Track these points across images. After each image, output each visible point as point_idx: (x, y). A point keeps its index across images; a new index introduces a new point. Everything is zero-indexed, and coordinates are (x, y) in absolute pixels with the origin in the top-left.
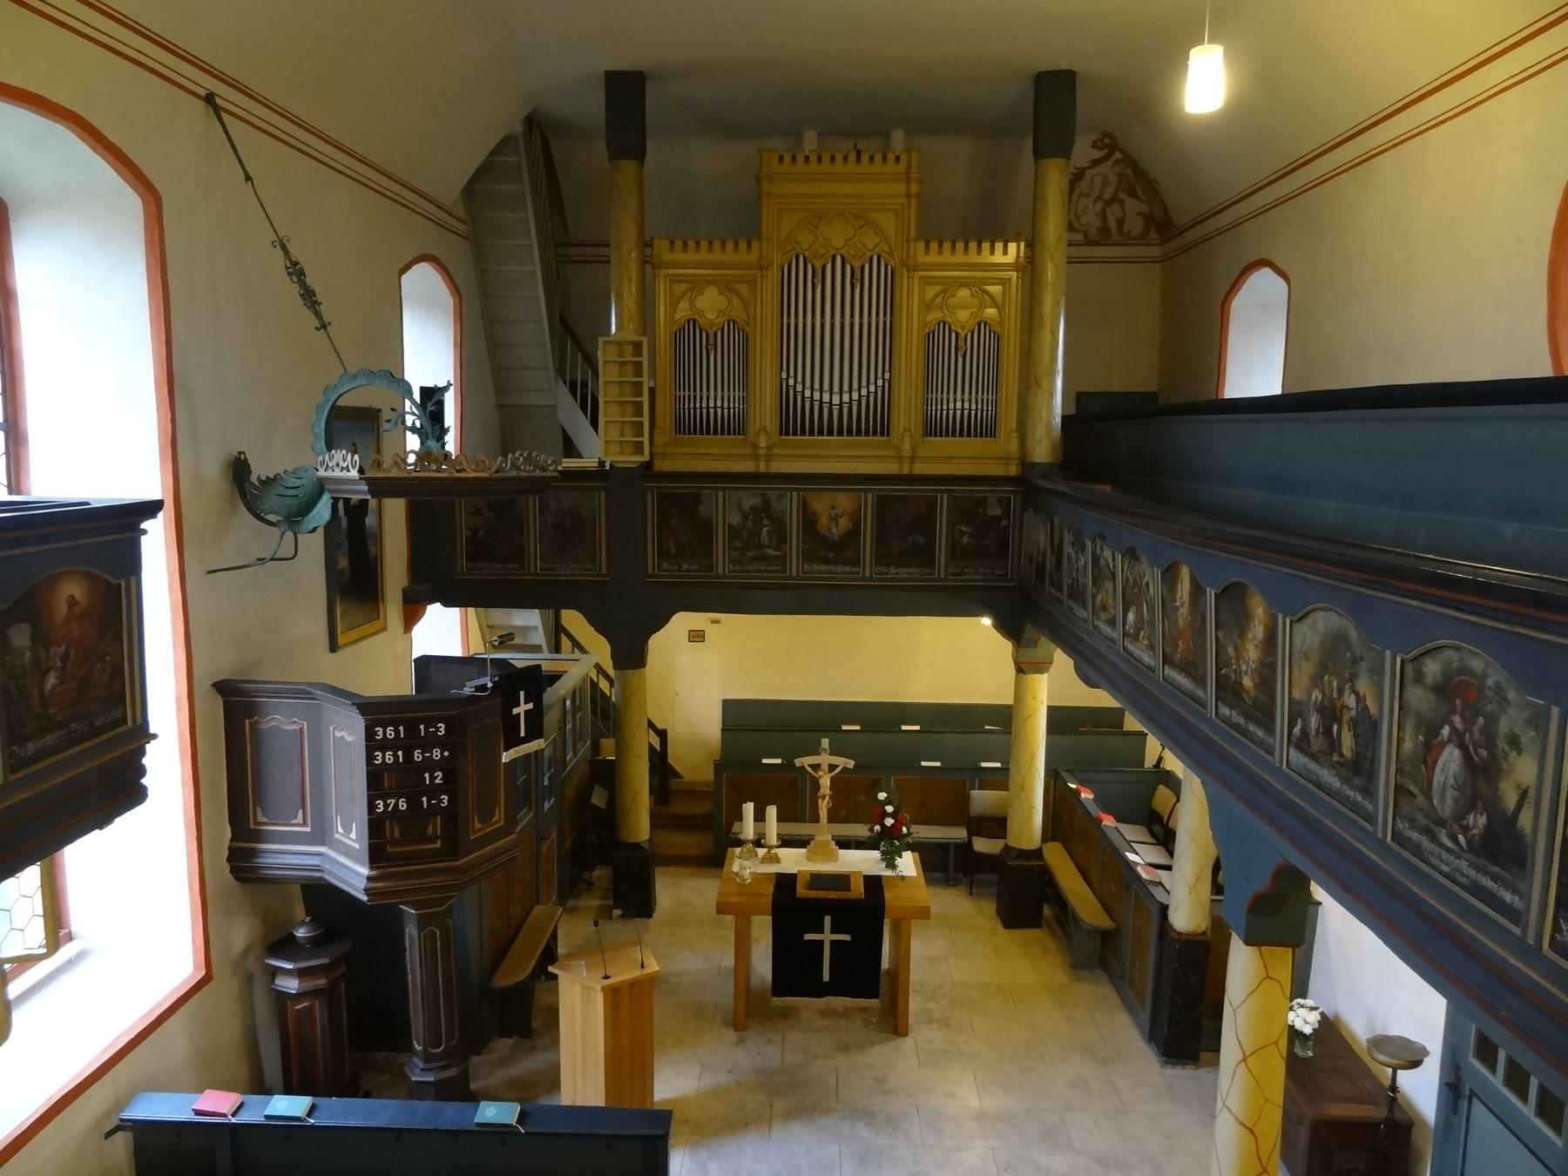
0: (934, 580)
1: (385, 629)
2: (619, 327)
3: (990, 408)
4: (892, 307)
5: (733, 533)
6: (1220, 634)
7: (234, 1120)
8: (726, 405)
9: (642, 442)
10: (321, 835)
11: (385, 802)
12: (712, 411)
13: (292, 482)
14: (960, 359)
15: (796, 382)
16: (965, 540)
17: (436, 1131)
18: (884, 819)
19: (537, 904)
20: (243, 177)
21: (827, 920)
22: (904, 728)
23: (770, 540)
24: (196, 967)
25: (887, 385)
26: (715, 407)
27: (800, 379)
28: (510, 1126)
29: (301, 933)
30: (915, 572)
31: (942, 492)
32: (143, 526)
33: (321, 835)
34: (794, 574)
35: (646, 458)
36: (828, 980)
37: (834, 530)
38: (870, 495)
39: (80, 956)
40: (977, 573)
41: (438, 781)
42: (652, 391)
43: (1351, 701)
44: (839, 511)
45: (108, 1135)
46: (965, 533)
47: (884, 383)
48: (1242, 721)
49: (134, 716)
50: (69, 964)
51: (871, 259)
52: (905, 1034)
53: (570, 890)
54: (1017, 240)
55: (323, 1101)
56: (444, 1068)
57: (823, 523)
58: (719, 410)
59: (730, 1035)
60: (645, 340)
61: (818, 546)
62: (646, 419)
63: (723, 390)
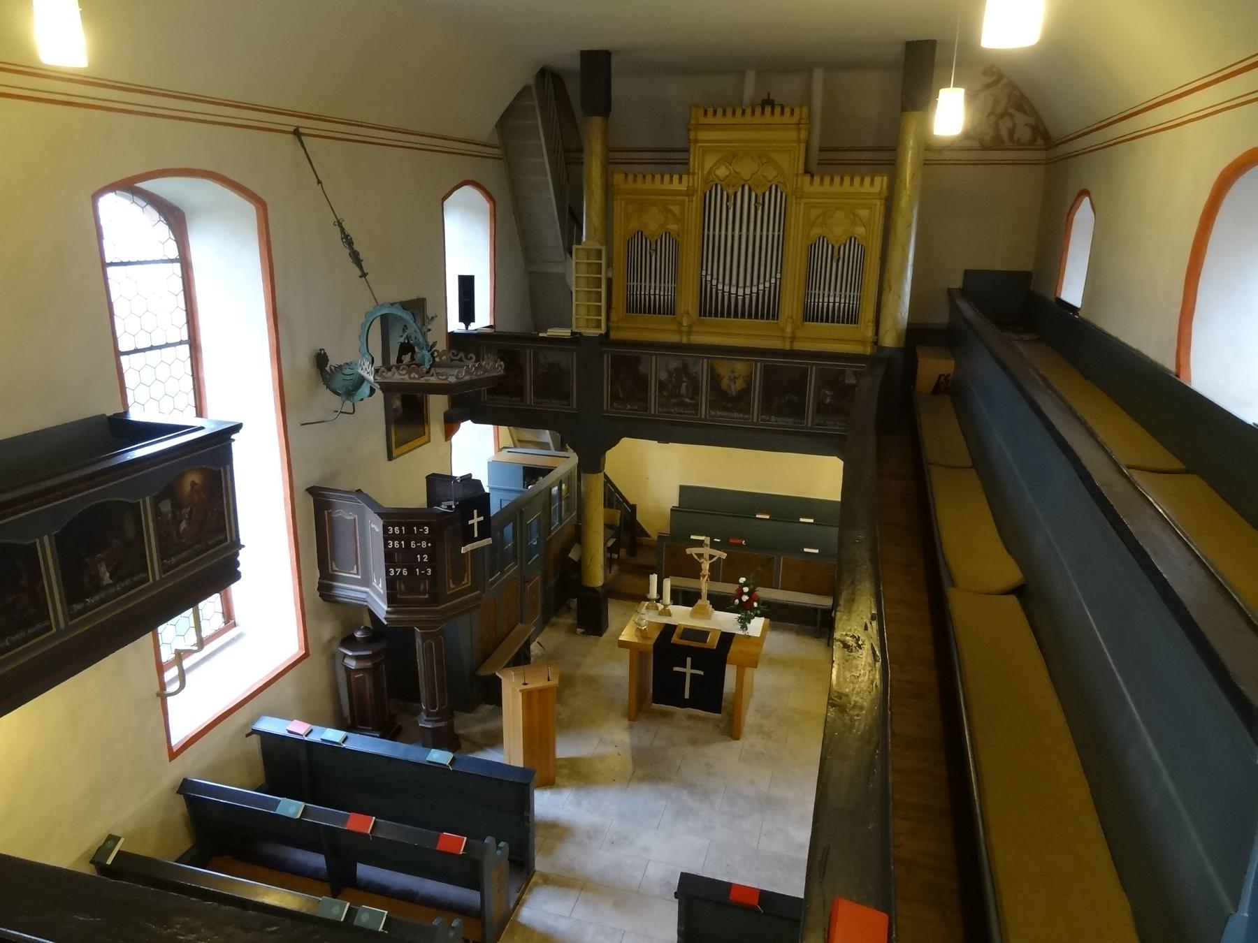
0: (803, 428)
1: (429, 441)
3: (855, 303)
4: (783, 225)
5: (662, 386)
7: (306, 739)
8: (662, 293)
9: (601, 320)
10: (366, 582)
11: (395, 570)
12: (652, 297)
13: (348, 371)
14: (834, 265)
15: (712, 278)
16: (828, 401)
17: (406, 761)
18: (742, 596)
19: (521, 623)
20: (317, 181)
21: (689, 660)
22: (802, 520)
23: (688, 393)
24: (300, 648)
25: (778, 282)
26: (655, 294)
27: (715, 276)
28: (445, 765)
29: (358, 634)
30: (790, 421)
31: (813, 364)
32: (233, 437)
33: (366, 582)
34: (703, 417)
35: (603, 331)
36: (688, 698)
37: (733, 388)
38: (759, 364)
39: (240, 636)
40: (834, 425)
41: (425, 560)
42: (609, 282)
44: (737, 375)
45: (248, 735)
46: (827, 395)
47: (776, 281)
49: (231, 537)
50: (233, 640)
51: (771, 188)
52: (737, 738)
53: (549, 615)
54: (882, 176)
55: (350, 735)
56: (437, 721)
57: (725, 383)
58: (657, 296)
59: (625, 722)
60: (603, 248)
61: (720, 397)
62: (603, 303)
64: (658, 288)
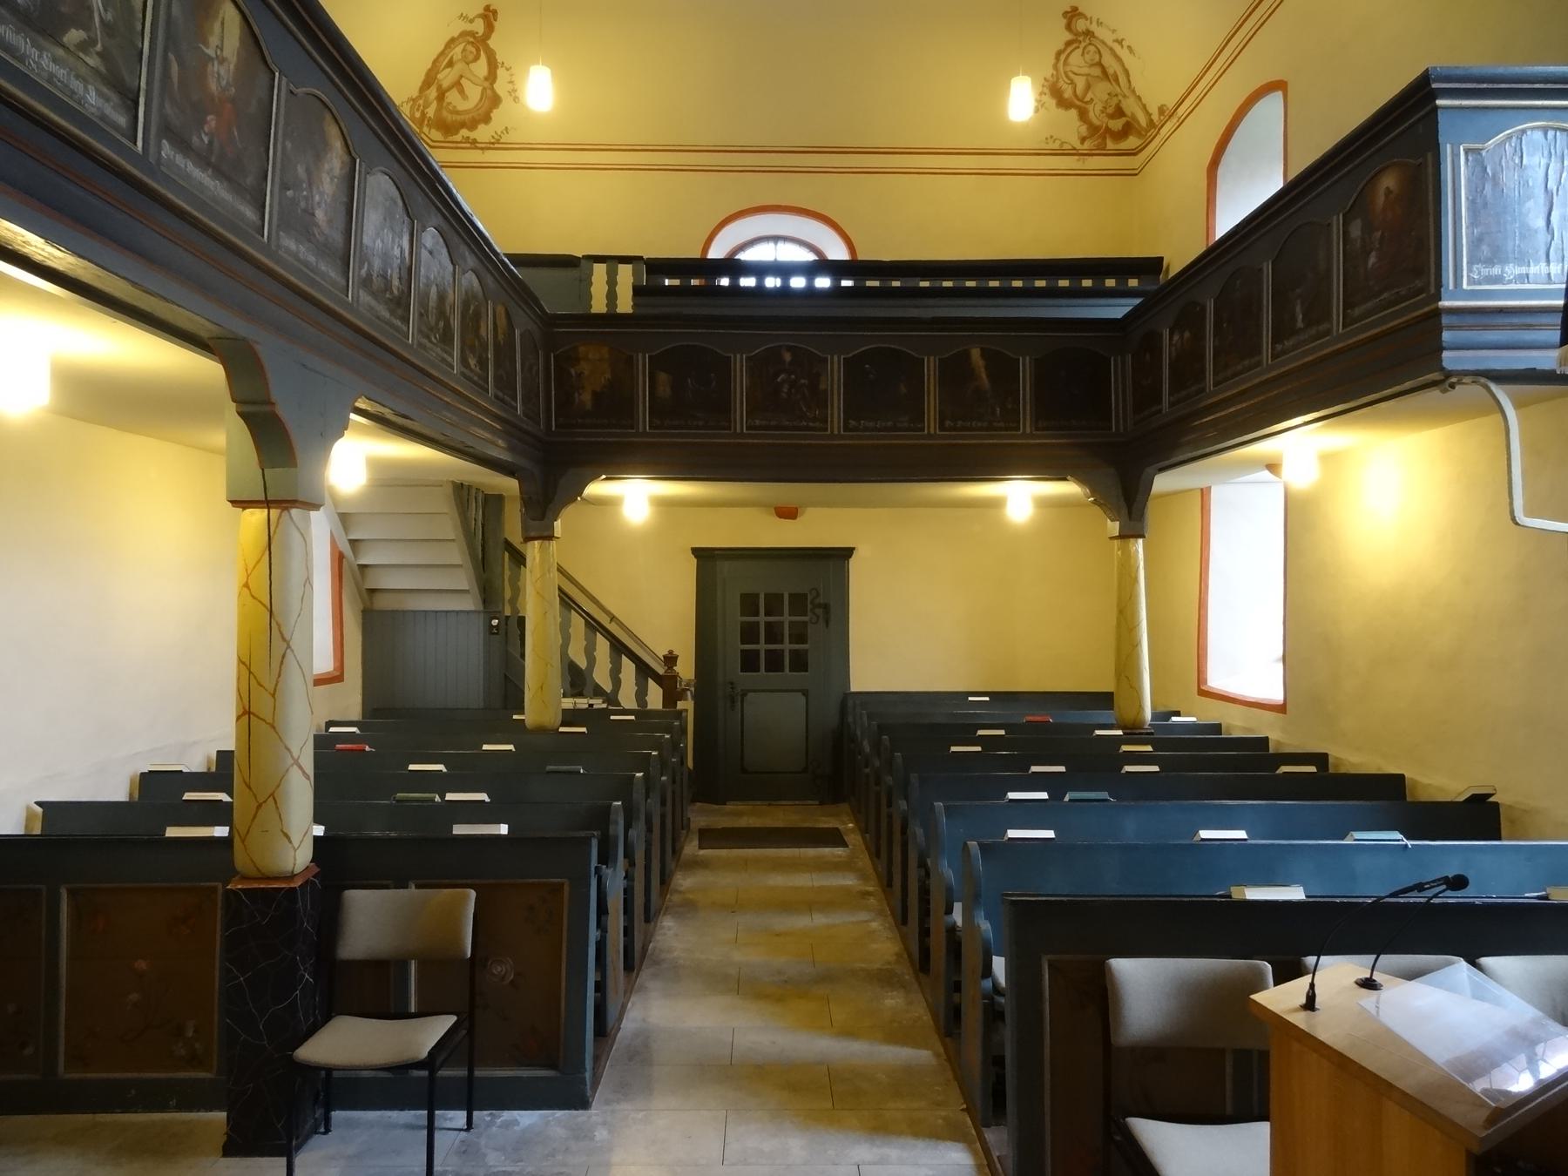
6: (289, 145)
43: (397, 252)
48: (312, 259)
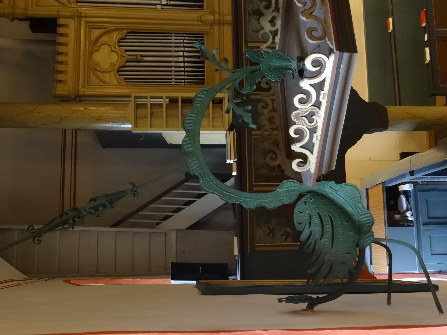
2: (125, 120)
63: (171, 51)
64: (176, 54)
